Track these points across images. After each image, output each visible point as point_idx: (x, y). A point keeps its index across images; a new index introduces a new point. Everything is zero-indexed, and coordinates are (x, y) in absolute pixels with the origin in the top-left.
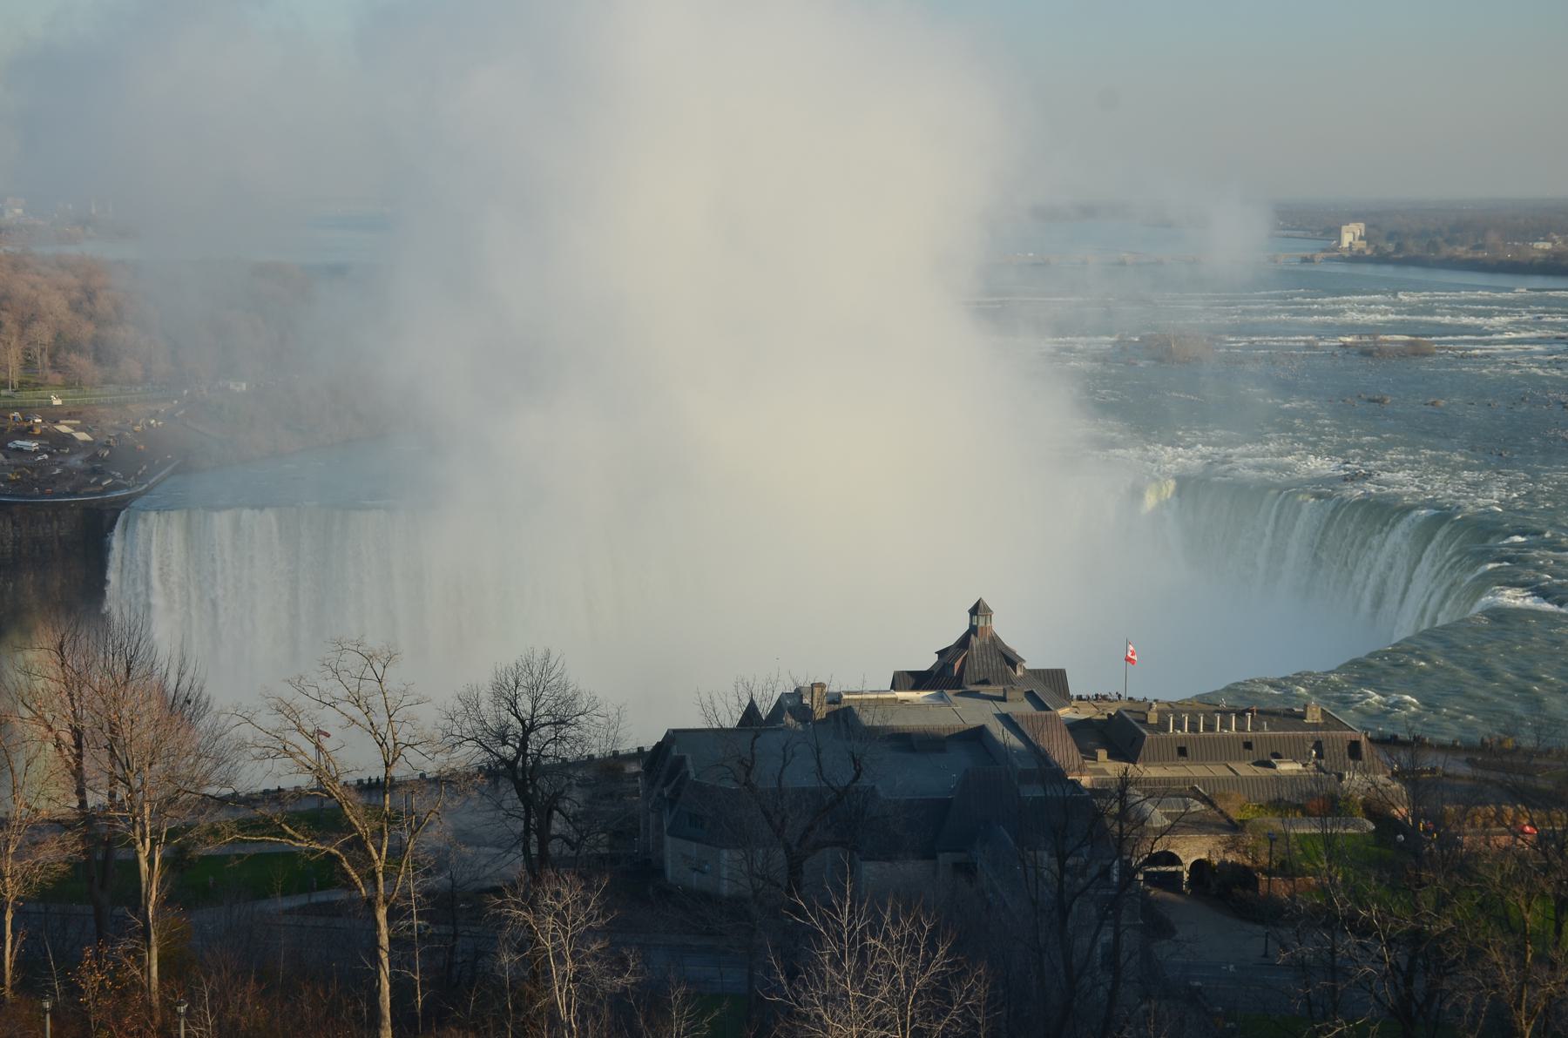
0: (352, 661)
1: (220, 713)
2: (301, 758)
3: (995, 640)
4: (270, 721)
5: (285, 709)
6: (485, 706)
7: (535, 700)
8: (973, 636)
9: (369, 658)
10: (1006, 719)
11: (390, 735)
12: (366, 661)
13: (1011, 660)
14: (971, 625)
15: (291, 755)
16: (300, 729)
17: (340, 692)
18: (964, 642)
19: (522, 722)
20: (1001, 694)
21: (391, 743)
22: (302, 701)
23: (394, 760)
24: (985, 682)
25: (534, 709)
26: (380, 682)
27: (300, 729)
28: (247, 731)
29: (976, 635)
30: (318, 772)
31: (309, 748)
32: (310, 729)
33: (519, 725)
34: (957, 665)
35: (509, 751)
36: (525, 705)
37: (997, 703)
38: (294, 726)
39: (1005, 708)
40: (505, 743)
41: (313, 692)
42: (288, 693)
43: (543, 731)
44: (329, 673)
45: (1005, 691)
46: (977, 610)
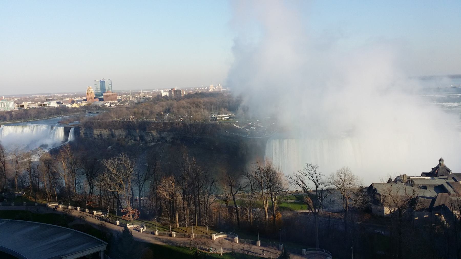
0: (310, 168)
1: (285, 177)
2: (300, 185)
3: (445, 166)
4: (295, 178)
5: (298, 176)
8: (440, 166)
10: (448, 183)
11: (317, 182)
13: (448, 171)
14: (439, 163)
15: (299, 185)
16: (300, 180)
17: (308, 173)
18: (437, 167)
19: (343, 180)
20: (446, 178)
21: (317, 183)
22: (300, 175)
23: (318, 186)
24: (443, 175)
26: (315, 172)
27: (300, 180)
28: (290, 180)
29: (440, 165)
30: (303, 188)
31: (301, 183)
32: (302, 180)
34: (436, 171)
35: (340, 186)
37: (445, 180)
38: (299, 179)
39: (447, 181)
41: (303, 173)
42: (298, 173)
45: (447, 177)
46: (440, 160)
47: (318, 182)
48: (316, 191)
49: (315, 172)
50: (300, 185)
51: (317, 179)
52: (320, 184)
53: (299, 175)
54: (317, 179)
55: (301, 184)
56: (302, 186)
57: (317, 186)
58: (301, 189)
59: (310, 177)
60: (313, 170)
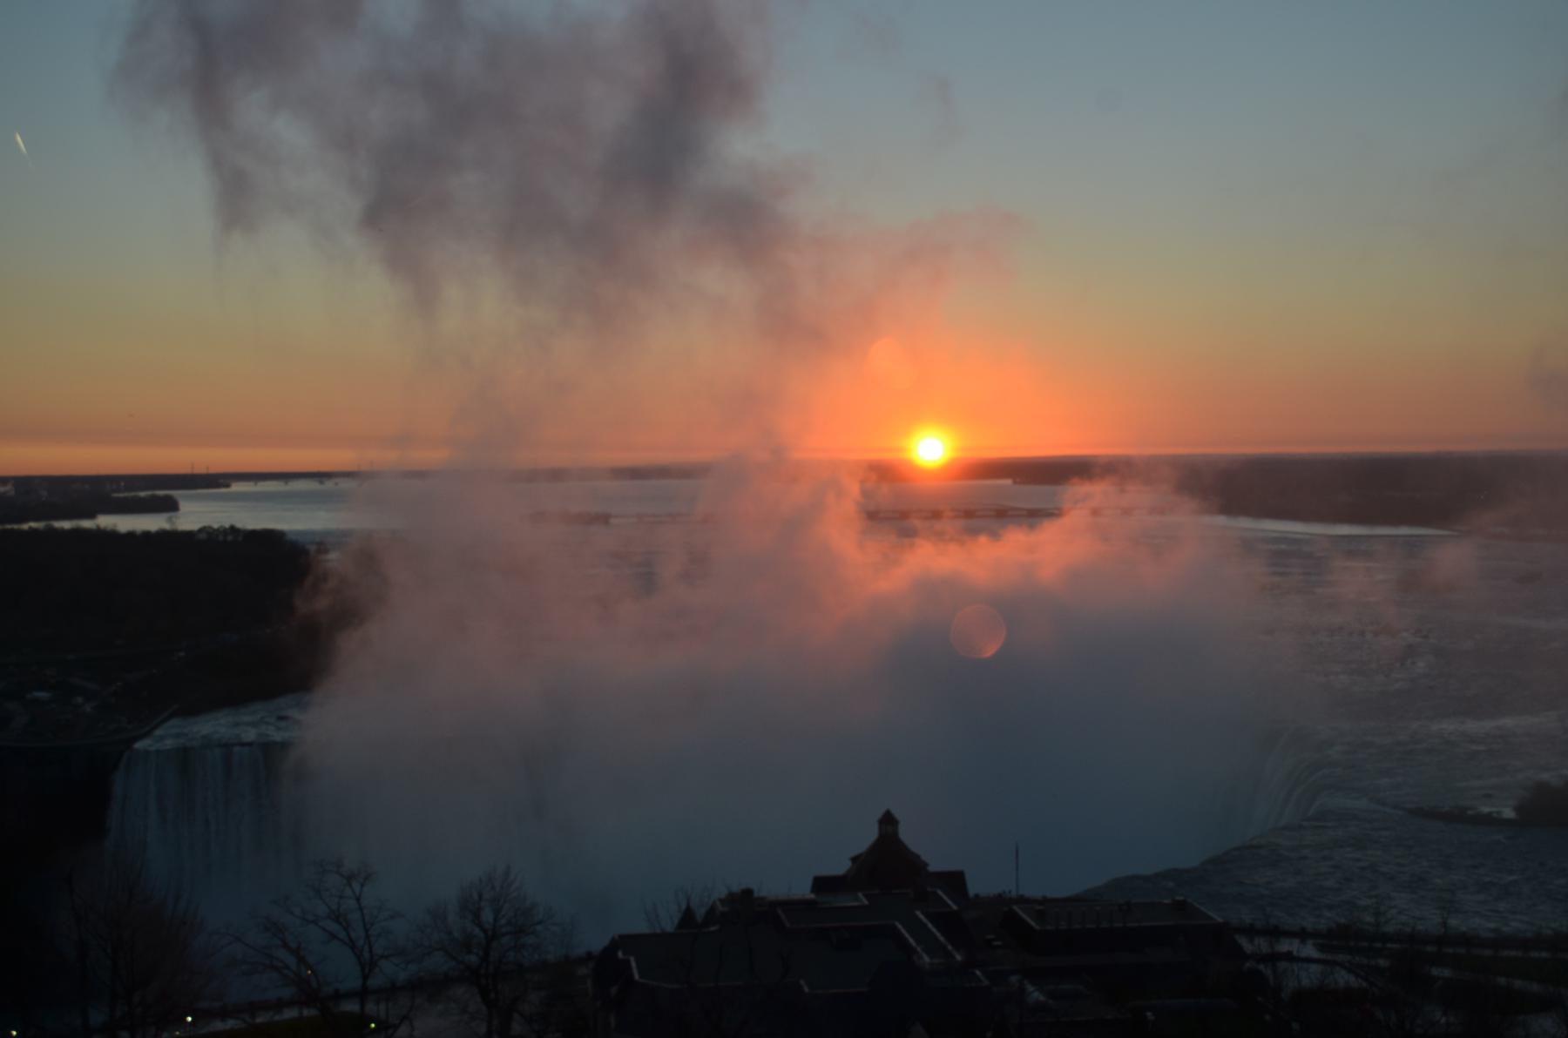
9: (350, 878)
11: (366, 948)
16: (285, 945)
19: (485, 931)
21: (366, 955)
25: (495, 920)
26: (358, 899)
27: (285, 945)
31: (291, 961)
33: (482, 935)
35: (473, 959)
36: (487, 916)
48: (363, 994)
49: (358, 899)
51: (368, 937)
52: (382, 957)
54: (368, 937)
57: (368, 967)
58: (287, 993)
59: (333, 926)
60: (348, 892)
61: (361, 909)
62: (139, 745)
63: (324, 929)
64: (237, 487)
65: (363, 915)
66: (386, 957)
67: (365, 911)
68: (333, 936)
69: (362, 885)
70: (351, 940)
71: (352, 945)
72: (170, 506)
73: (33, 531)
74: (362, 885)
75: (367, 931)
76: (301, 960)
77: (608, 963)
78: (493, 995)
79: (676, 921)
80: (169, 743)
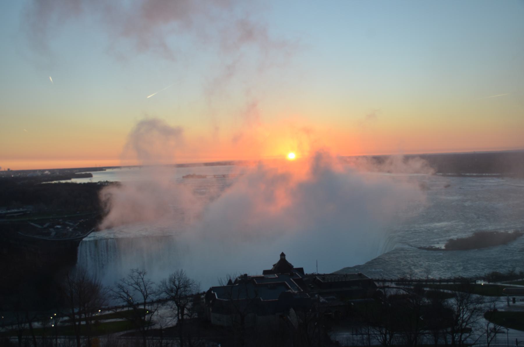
0: (136, 274)
2: (124, 298)
4: (117, 290)
5: (121, 287)
6: (167, 283)
7: (179, 282)
9: (140, 273)
11: (145, 292)
12: (139, 274)
15: (122, 297)
16: (124, 291)
17: (133, 282)
19: (176, 287)
22: (124, 285)
23: (146, 297)
25: (179, 284)
26: (142, 279)
27: (124, 291)
28: (111, 293)
31: (126, 295)
32: (126, 291)
33: (175, 288)
35: (173, 294)
36: (177, 283)
38: (122, 290)
40: (172, 292)
41: (127, 282)
43: (182, 289)
44: (130, 278)
47: (146, 292)
48: (145, 304)
49: (142, 279)
50: (124, 298)
51: (145, 289)
52: (149, 294)
53: (123, 285)
54: (145, 289)
55: (124, 297)
56: (126, 299)
57: (146, 297)
58: (125, 304)
60: (140, 277)
61: (143, 281)
62: (84, 239)
63: (134, 287)
64: (108, 170)
65: (144, 283)
66: (151, 294)
67: (144, 282)
68: (136, 289)
69: (143, 275)
70: (141, 289)
71: (141, 291)
72: (90, 176)
73: (55, 184)
74: (143, 275)
75: (145, 287)
76: (128, 295)
77: (209, 294)
78: (179, 303)
79: (227, 283)
80: (92, 239)
